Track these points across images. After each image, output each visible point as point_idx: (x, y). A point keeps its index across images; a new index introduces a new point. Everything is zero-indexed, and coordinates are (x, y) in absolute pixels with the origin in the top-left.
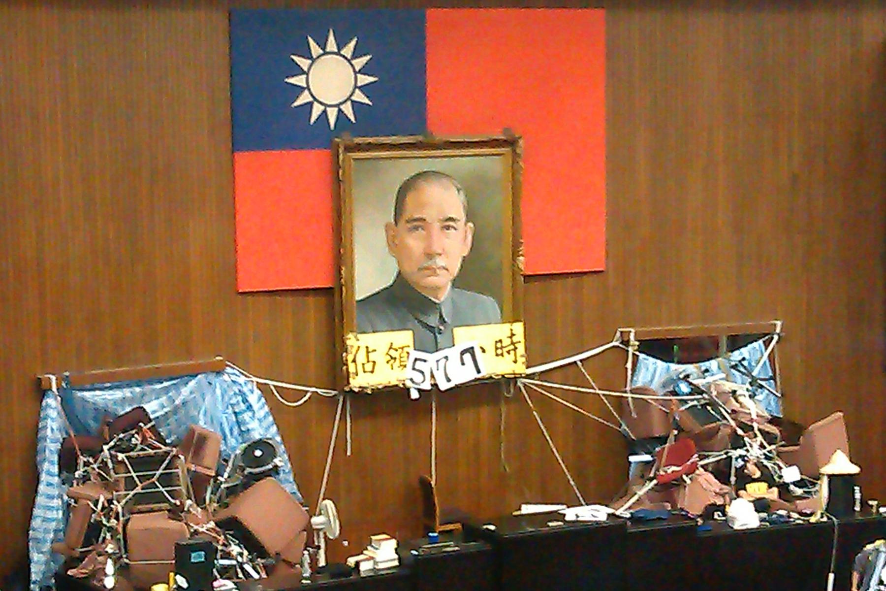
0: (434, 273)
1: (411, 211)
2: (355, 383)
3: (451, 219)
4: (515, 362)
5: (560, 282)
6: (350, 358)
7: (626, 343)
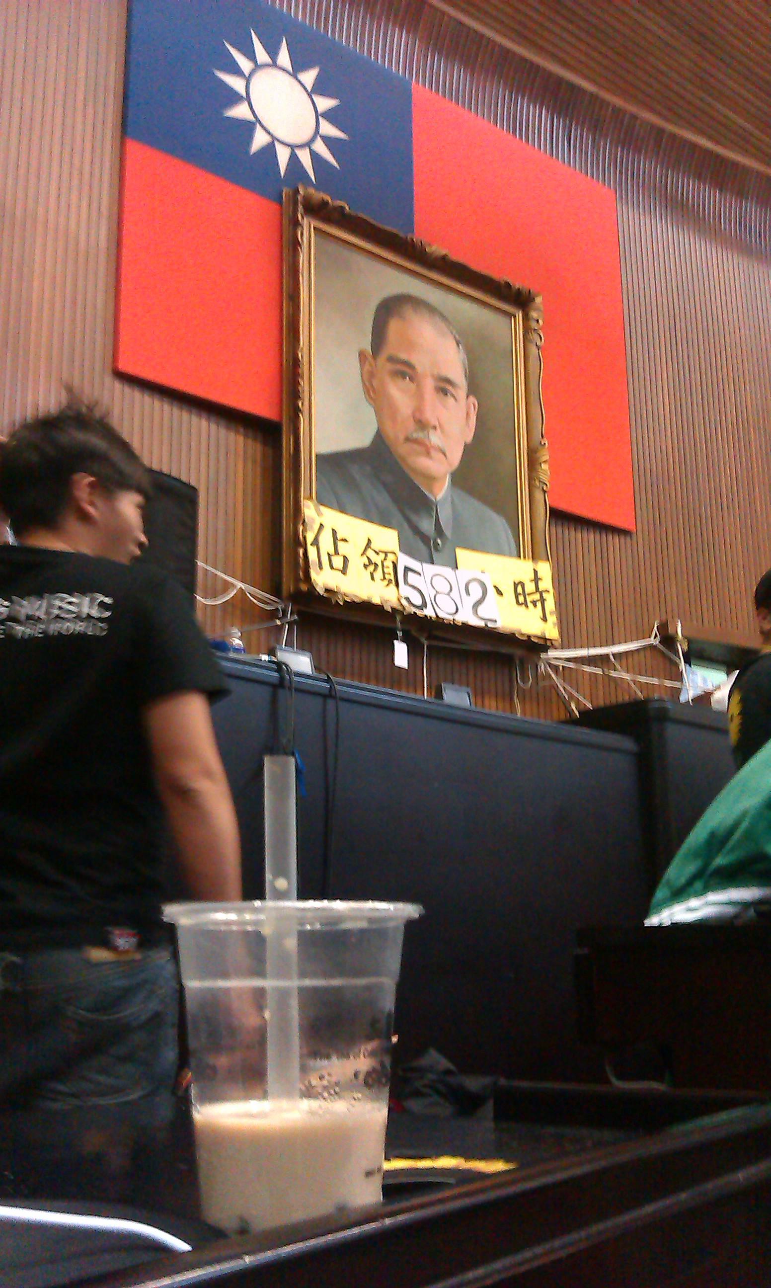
0: (428, 454)
3: (448, 381)
4: (545, 619)
6: (310, 537)
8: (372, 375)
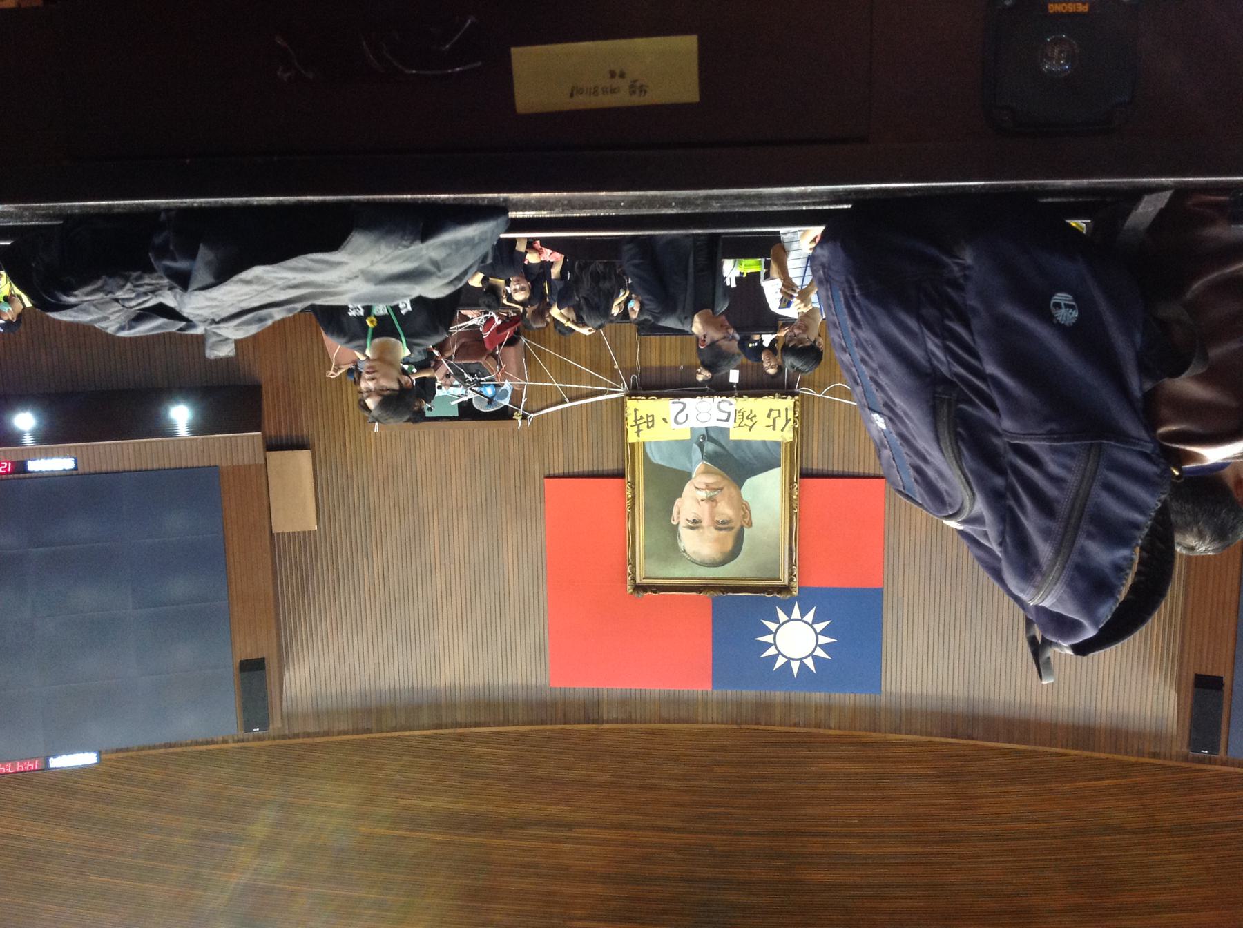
0: (707, 485)
1: (729, 539)
2: (789, 402)
3: (692, 528)
4: (636, 410)
5: (586, 469)
6: (791, 423)
7: (524, 417)
8: (744, 516)
